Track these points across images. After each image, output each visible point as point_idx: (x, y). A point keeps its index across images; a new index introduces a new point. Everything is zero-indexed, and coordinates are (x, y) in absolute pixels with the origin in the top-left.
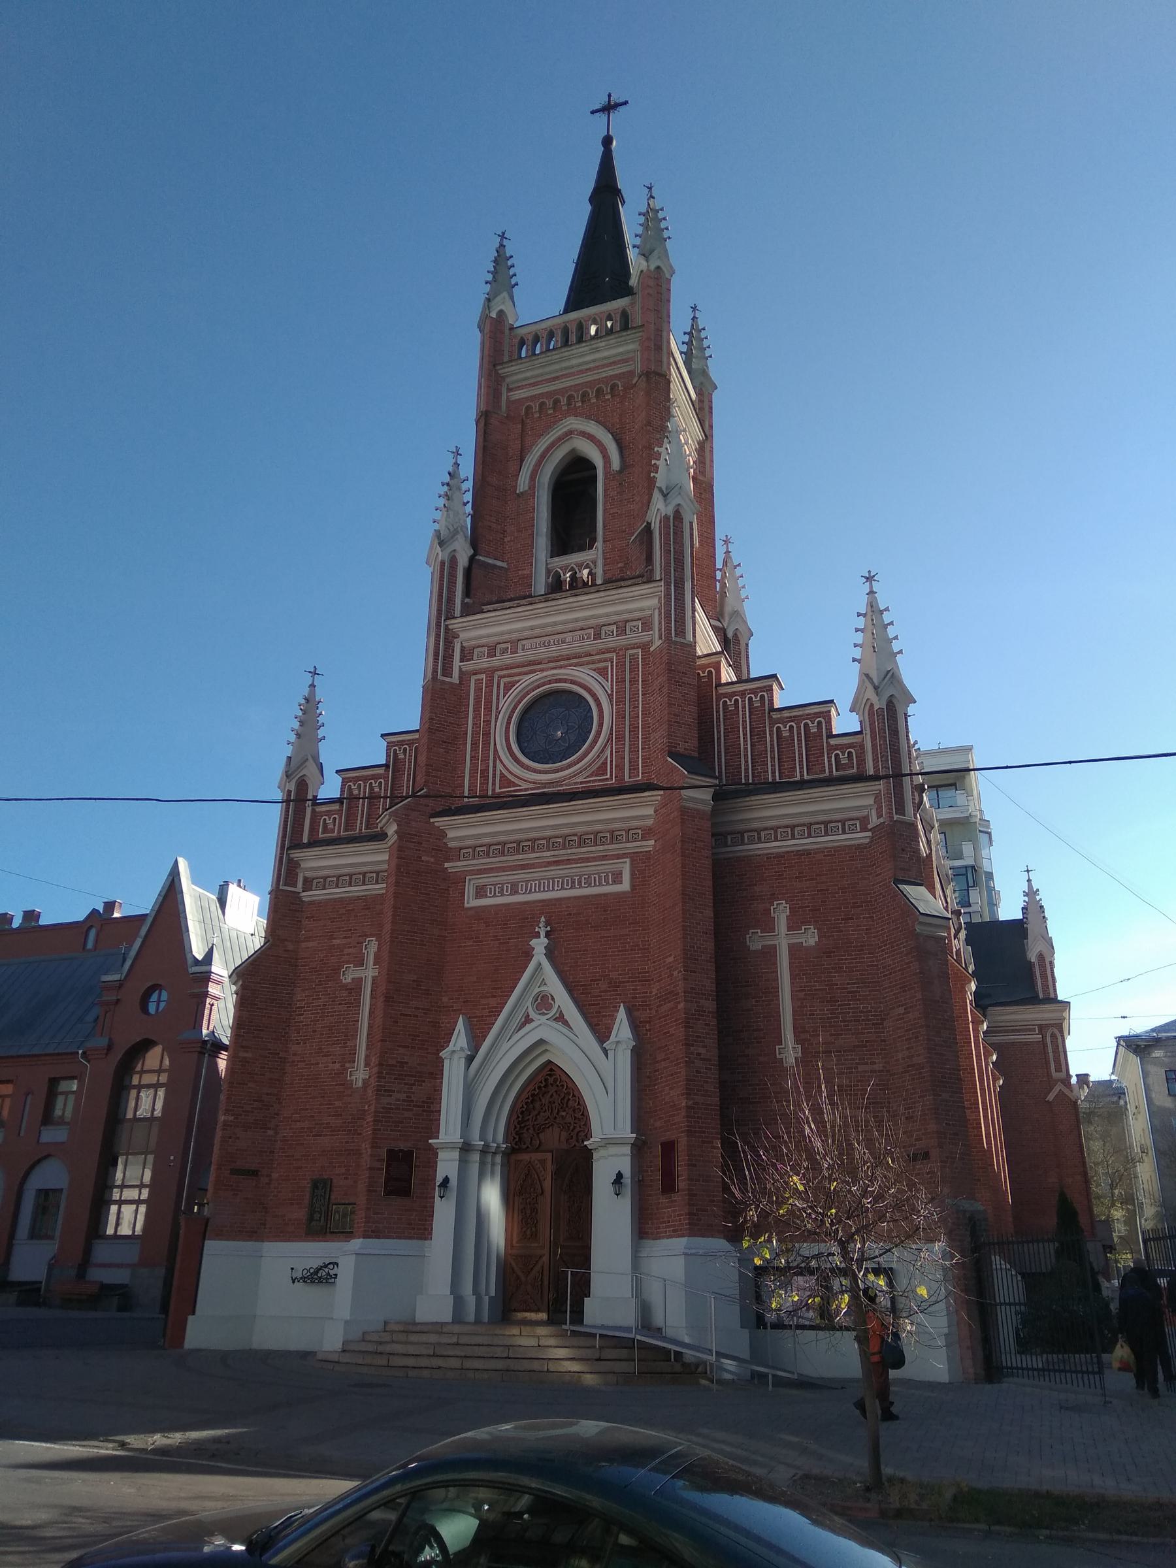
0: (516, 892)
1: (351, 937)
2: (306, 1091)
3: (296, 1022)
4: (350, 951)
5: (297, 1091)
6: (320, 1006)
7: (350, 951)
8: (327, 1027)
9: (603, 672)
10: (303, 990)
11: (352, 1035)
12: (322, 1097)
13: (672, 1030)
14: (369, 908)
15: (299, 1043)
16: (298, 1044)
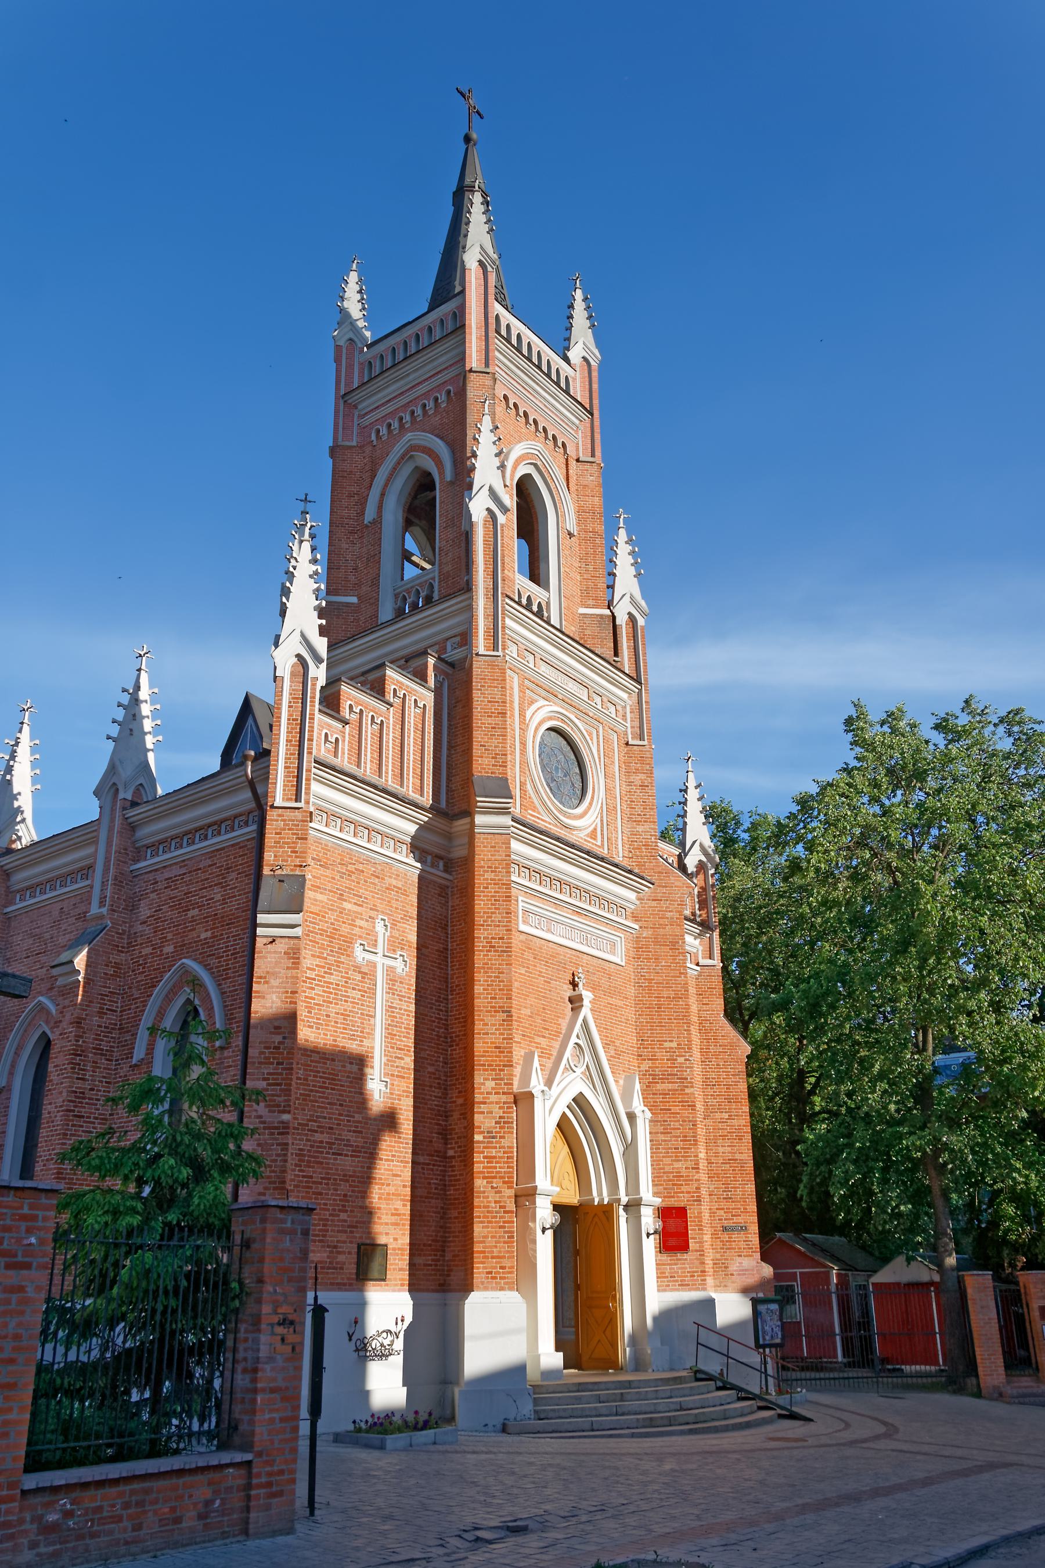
0: (549, 931)
1: (361, 906)
2: (324, 1093)
3: (306, 997)
4: (363, 923)
5: (312, 1091)
6: (332, 983)
7: (363, 923)
8: (342, 1014)
9: (590, 734)
10: (313, 956)
11: (368, 1033)
12: (341, 1105)
13: (675, 1109)
14: (378, 877)
15: (312, 1027)
16: (310, 1027)
